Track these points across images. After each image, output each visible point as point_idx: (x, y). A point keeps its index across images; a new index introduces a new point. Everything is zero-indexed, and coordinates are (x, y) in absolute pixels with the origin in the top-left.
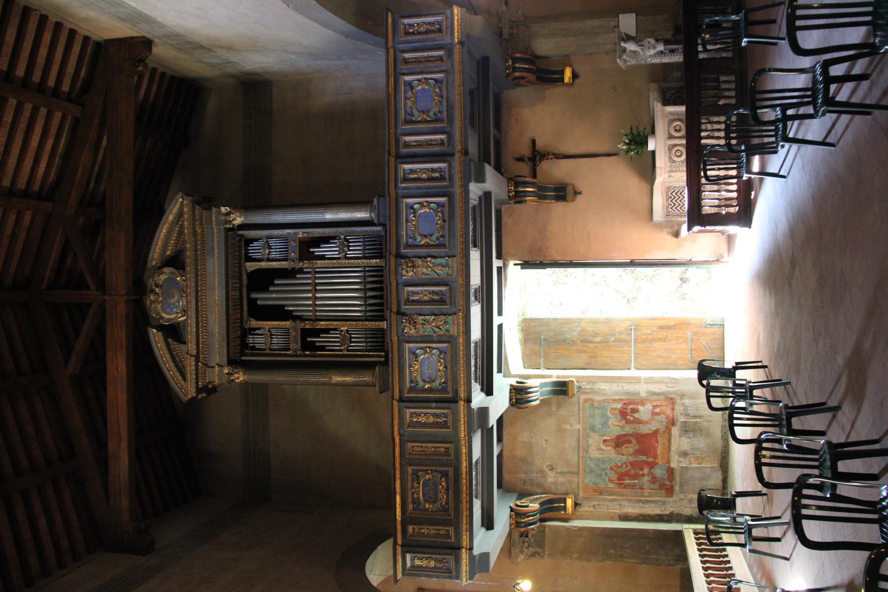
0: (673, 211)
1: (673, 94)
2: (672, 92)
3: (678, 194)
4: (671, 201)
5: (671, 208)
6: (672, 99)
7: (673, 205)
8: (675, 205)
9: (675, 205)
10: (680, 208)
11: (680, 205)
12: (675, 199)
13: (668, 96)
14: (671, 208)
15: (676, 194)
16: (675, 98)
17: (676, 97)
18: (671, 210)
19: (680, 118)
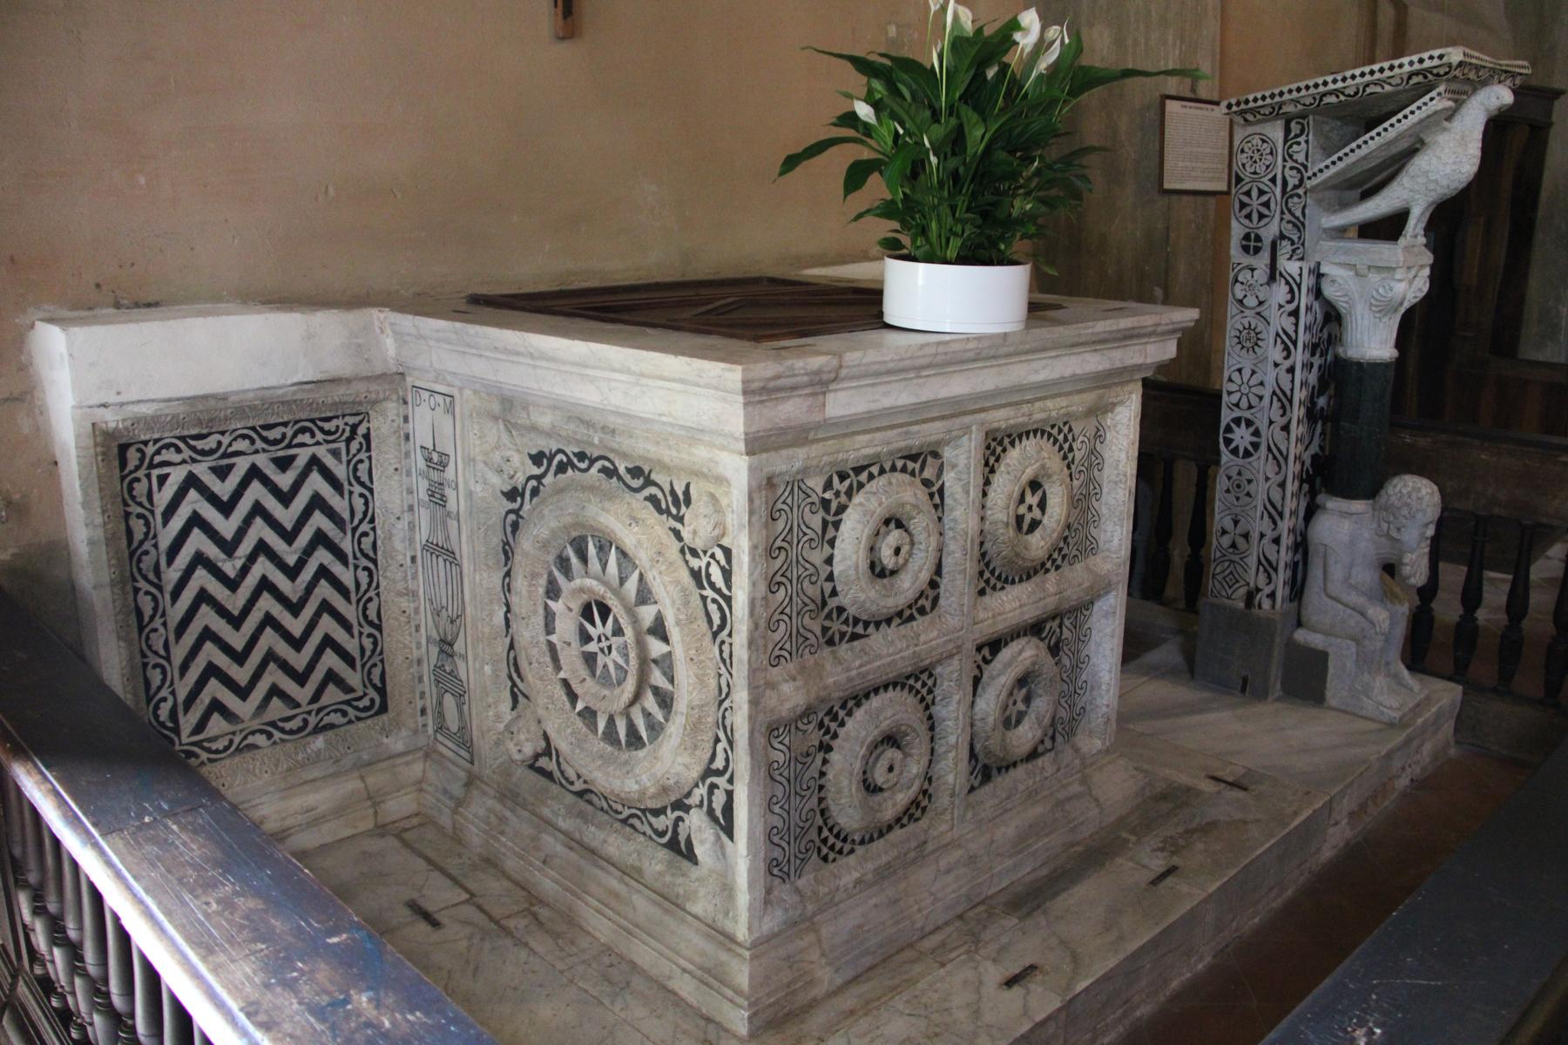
0: (163, 498)
3: (319, 520)
4: (254, 473)
5: (192, 481)
7: (224, 489)
8: (226, 508)
9: (226, 508)
10: (199, 559)
11: (229, 548)
12: (271, 504)
14: (192, 481)
15: (317, 502)
18: (177, 476)
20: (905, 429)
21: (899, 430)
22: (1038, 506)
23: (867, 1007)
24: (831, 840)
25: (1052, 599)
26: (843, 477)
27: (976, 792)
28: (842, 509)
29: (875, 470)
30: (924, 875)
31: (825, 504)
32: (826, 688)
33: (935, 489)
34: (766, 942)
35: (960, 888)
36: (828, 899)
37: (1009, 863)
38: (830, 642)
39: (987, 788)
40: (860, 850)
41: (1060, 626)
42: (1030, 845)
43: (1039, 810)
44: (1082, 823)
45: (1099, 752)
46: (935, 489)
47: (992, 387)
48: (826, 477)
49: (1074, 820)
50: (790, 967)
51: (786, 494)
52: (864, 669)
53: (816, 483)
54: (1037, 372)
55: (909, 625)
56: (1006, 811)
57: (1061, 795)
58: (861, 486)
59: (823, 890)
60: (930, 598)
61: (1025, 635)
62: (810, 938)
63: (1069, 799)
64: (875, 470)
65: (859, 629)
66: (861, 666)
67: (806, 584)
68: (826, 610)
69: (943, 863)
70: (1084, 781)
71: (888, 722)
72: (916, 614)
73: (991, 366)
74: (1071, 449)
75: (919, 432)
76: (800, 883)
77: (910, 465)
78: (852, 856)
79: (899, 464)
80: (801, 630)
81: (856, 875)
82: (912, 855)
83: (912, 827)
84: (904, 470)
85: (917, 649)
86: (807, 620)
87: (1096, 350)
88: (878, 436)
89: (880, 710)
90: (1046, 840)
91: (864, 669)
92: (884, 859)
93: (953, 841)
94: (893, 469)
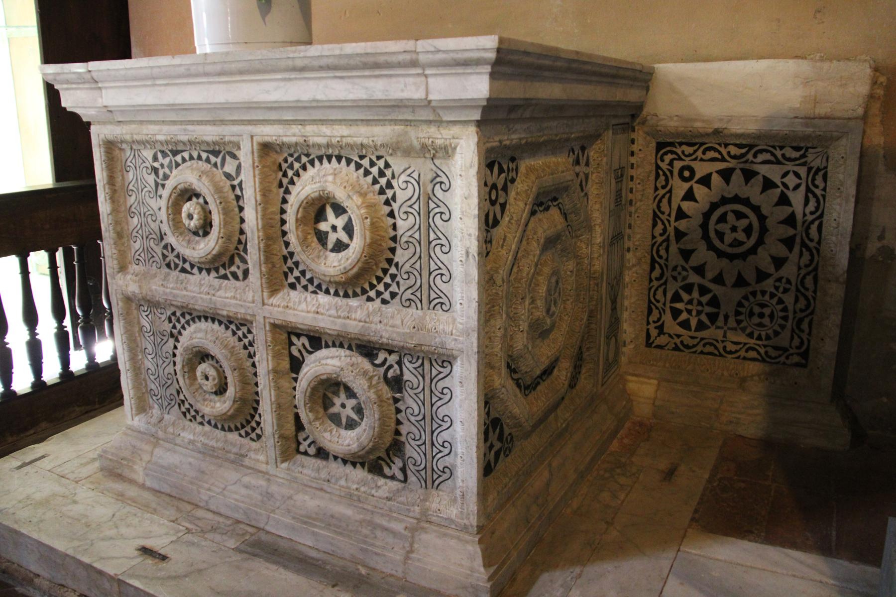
1: (784, 200)
2: (797, 198)
6: (753, 192)
13: (773, 173)
16: (756, 209)
17: (762, 218)
19: (401, 256)
20: (184, 127)
21: (180, 127)
22: (344, 229)
23: (145, 507)
24: (248, 429)
25: (355, 323)
26: (165, 155)
27: (308, 458)
28: (166, 177)
29: (186, 155)
30: (230, 475)
31: (155, 171)
32: (151, 291)
33: (236, 183)
34: (132, 430)
35: (243, 502)
36: (171, 437)
37: (288, 520)
38: (168, 266)
39: (319, 463)
40: (207, 428)
41: (400, 363)
42: (315, 526)
43: (349, 512)
44: (376, 554)
45: (452, 521)
46: (236, 183)
47: (223, 101)
48: (152, 152)
49: (372, 545)
50: (133, 453)
51: (132, 157)
52: (175, 291)
53: (148, 154)
54: (268, 92)
55: (222, 281)
56: (322, 489)
57: (378, 520)
58: (177, 165)
59: (171, 430)
60: (241, 269)
61: (350, 348)
62: (148, 448)
63: (385, 529)
64: (186, 155)
65: (187, 266)
66: (172, 288)
67: (149, 219)
68: (163, 243)
69: (246, 479)
70: (413, 530)
71: (197, 340)
72: (229, 275)
73: (219, 82)
74: (389, 185)
75: (194, 131)
76: (166, 417)
77: (213, 159)
78: (201, 427)
79: (204, 155)
80: (150, 249)
81: (191, 437)
82: (232, 456)
83: (246, 441)
84: (208, 160)
85: (214, 298)
86: (152, 244)
87: (341, 78)
88: (166, 128)
89: (200, 330)
90: (335, 536)
91: (175, 291)
92: (213, 443)
93: (267, 473)
94: (200, 158)
